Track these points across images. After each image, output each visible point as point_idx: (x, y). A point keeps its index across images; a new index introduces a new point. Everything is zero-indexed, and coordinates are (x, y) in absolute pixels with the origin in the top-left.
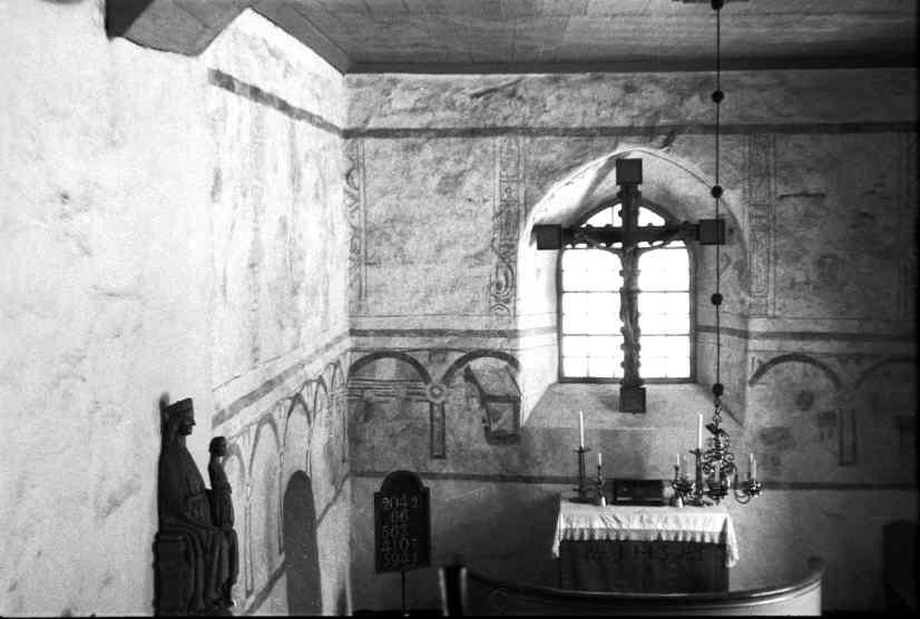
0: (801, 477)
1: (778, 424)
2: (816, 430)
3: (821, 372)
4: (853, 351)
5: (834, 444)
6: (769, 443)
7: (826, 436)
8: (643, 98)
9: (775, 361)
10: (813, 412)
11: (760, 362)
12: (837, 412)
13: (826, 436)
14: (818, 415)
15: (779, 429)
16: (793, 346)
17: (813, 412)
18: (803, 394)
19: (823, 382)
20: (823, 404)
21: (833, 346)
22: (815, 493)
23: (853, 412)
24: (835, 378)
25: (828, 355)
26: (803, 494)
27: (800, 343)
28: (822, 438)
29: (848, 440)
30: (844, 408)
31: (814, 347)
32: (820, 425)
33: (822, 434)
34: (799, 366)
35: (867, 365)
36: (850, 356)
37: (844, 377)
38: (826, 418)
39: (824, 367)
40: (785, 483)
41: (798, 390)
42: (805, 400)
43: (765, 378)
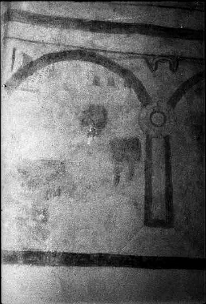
0: (83, 245)
1: (52, 155)
2: (109, 165)
3: (120, 80)
4: (168, 50)
5: (138, 188)
6: (32, 184)
7: (123, 178)
8: (48, 48)
9: (51, 58)
10: (106, 138)
11: (25, 55)
12: (143, 141)
13: (123, 178)
14: (112, 144)
15: (49, 163)
16: (79, 38)
17: (106, 138)
18: (91, 109)
19: (122, 94)
20: (123, 126)
21: (137, 43)
22: (105, 272)
23: (167, 139)
24: (141, 91)
25: (131, 55)
26: (81, 275)
27: (89, 36)
28: (118, 179)
29: (159, 187)
30: (151, 133)
31: (108, 43)
32: (118, 159)
33: (117, 172)
34: (87, 67)
35: (187, 72)
36: (164, 58)
37: (151, 86)
38: (126, 150)
39: (124, 72)
40: (55, 255)
41: (83, 103)
42: (95, 119)
43: (32, 81)
